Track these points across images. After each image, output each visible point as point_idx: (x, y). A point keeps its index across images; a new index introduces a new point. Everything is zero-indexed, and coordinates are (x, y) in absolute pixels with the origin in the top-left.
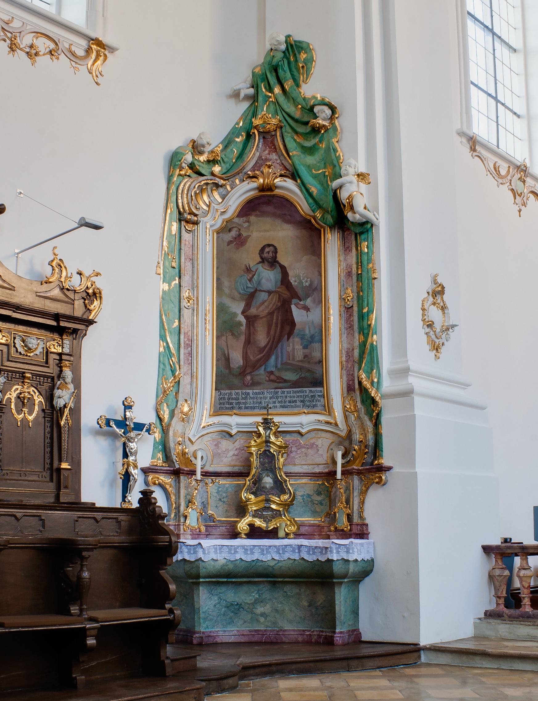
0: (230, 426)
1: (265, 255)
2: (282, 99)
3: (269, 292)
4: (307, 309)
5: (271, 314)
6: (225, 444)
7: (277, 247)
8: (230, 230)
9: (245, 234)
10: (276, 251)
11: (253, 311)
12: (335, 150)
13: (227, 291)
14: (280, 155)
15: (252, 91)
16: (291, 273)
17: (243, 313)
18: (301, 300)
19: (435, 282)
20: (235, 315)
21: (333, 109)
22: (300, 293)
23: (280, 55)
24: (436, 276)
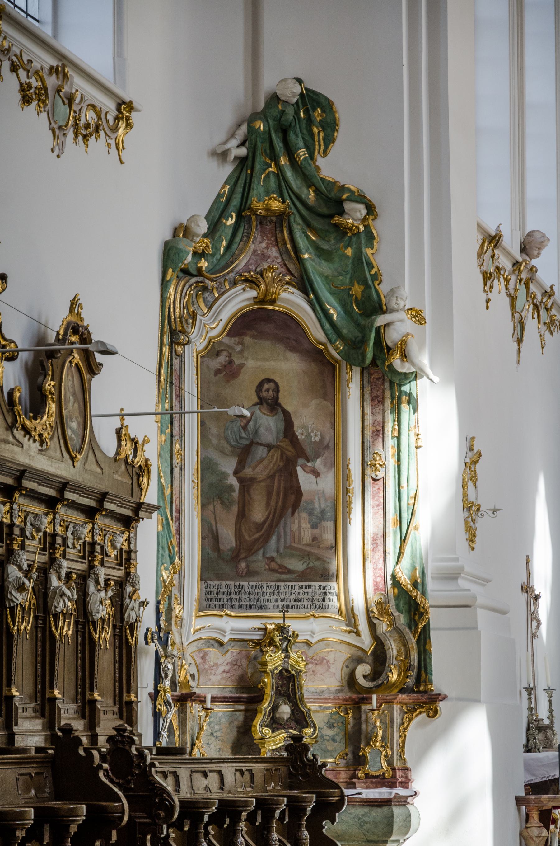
0: (223, 632)
1: (264, 394)
2: (289, 173)
3: (269, 447)
4: (317, 474)
5: (271, 477)
6: (214, 653)
7: (280, 384)
8: (218, 354)
9: (237, 362)
10: (277, 390)
11: (248, 472)
12: (370, 266)
13: (214, 441)
14: (284, 252)
15: (243, 151)
16: (297, 423)
17: (235, 473)
18: (308, 461)
19: (471, 449)
20: (225, 476)
21: (371, 209)
22: (308, 450)
23: (290, 111)
24: (473, 439)
